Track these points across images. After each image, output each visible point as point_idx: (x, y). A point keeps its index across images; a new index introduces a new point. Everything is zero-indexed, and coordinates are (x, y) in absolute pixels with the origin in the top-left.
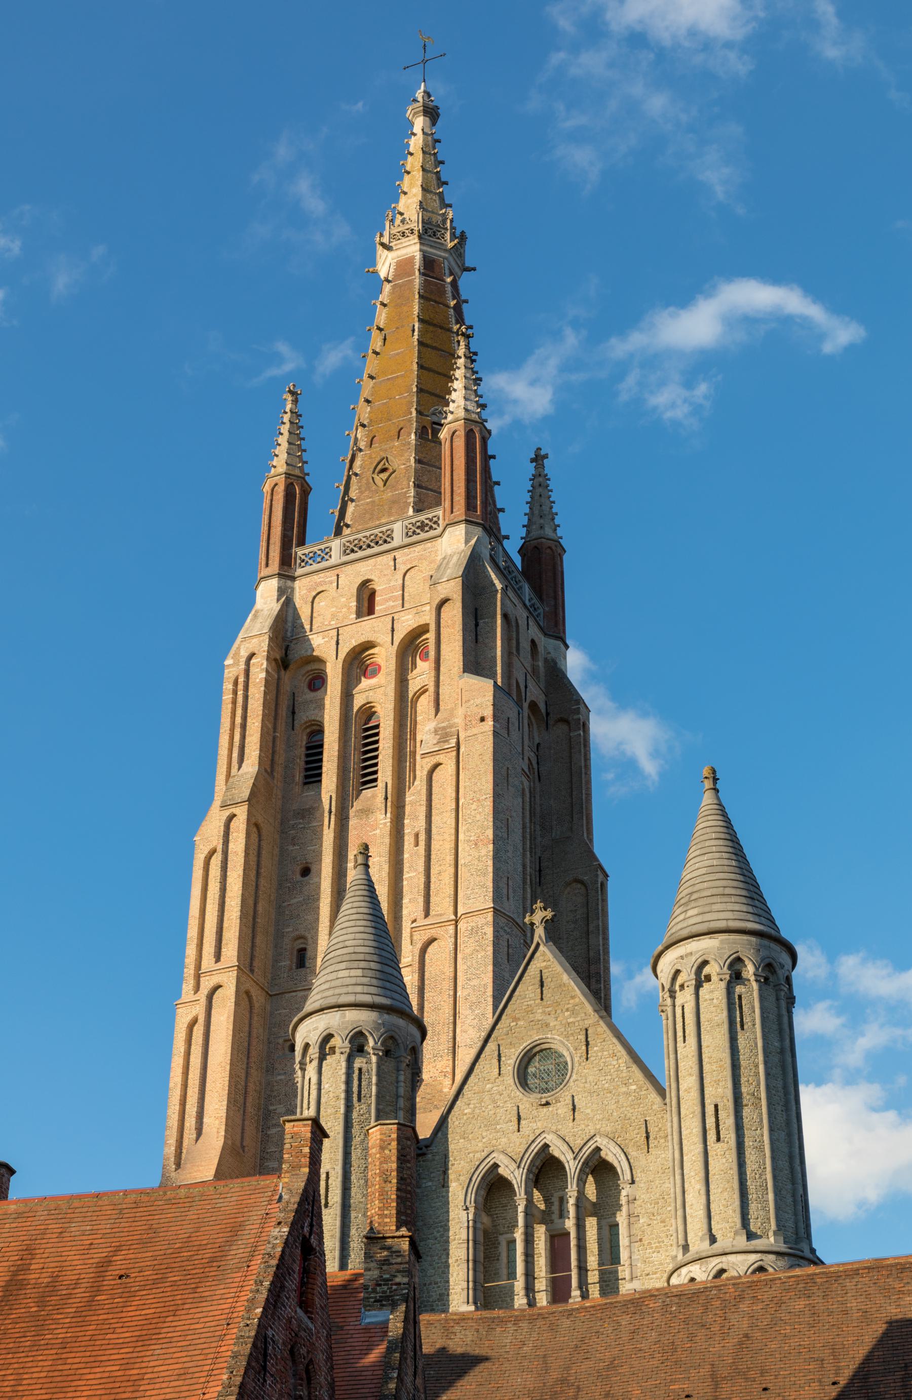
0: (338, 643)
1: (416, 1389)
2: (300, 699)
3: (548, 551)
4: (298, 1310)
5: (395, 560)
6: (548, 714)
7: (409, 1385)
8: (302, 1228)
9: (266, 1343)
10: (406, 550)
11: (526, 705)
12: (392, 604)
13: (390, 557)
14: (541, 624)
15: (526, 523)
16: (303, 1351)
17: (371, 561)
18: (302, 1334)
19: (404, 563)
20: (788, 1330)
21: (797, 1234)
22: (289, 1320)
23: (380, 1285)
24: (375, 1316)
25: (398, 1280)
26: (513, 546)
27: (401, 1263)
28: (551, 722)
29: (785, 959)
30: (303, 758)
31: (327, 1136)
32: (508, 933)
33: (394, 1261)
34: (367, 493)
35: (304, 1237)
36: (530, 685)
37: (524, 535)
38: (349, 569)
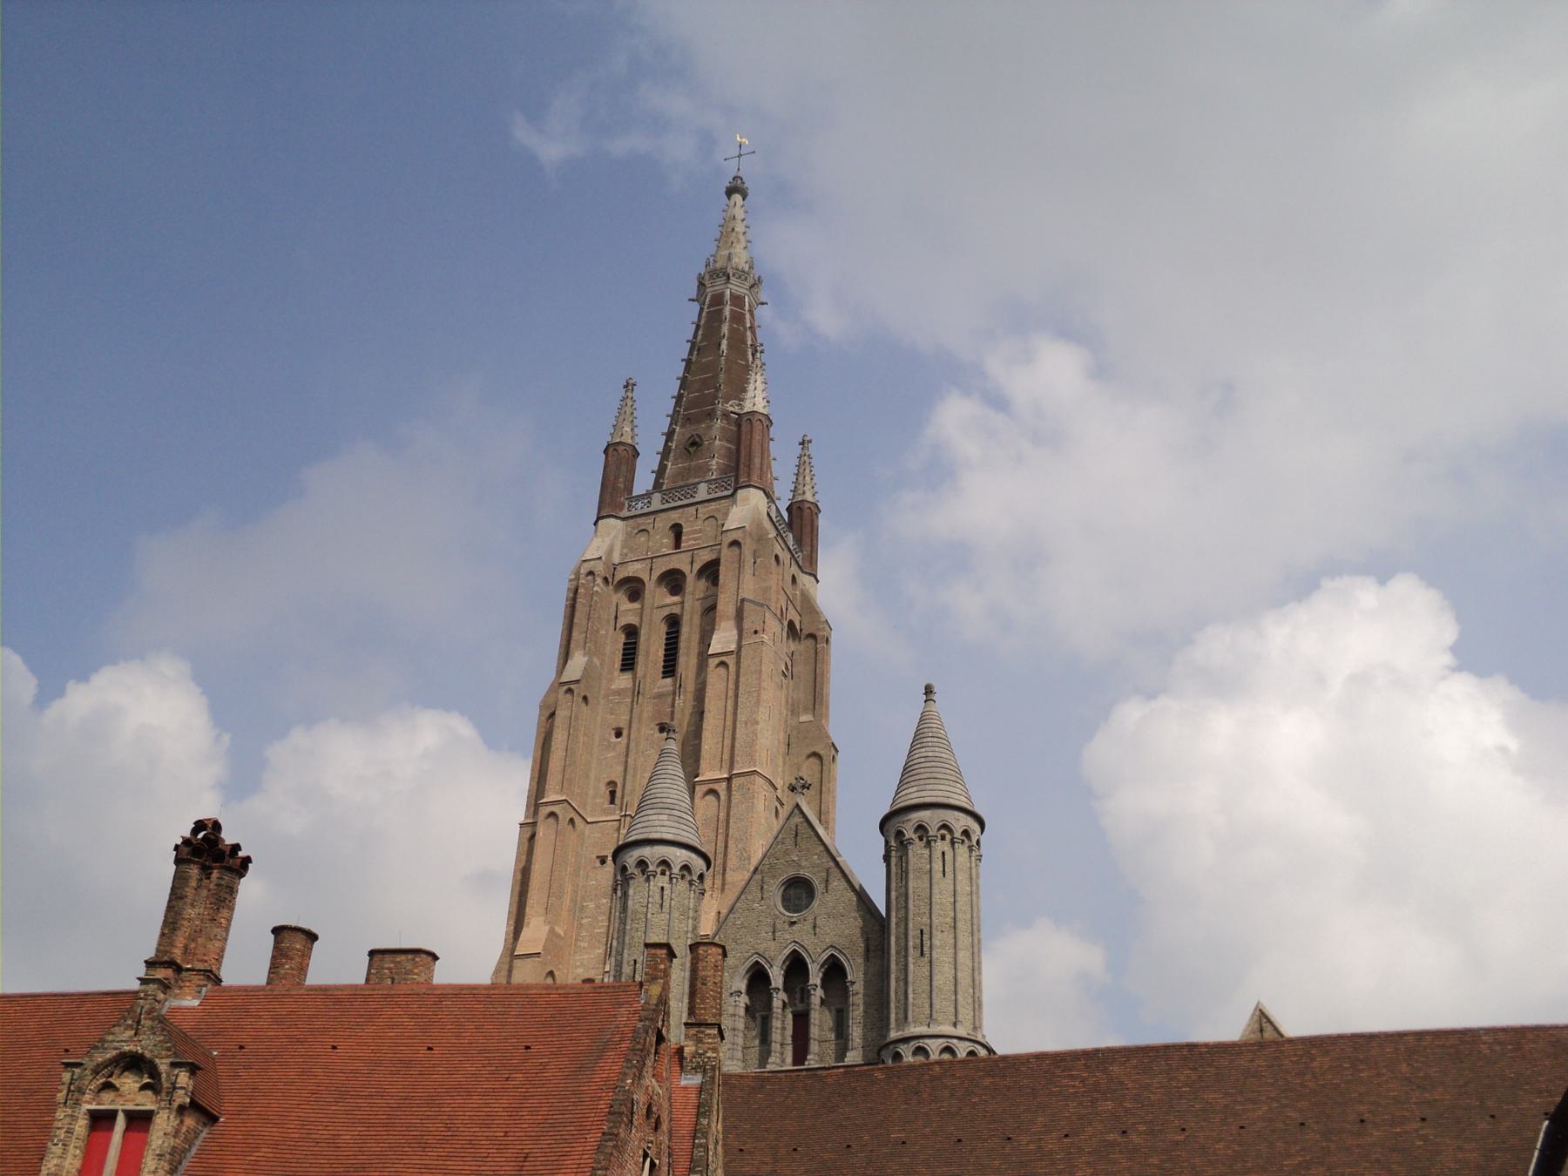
0: (651, 569)
1: (718, 1132)
2: (622, 608)
3: (808, 510)
4: (653, 1080)
5: (697, 510)
6: (801, 630)
7: (714, 1129)
8: (658, 1022)
9: (633, 1104)
10: (706, 504)
11: (786, 623)
12: (694, 542)
13: (694, 508)
14: (800, 563)
15: (793, 489)
16: (654, 1109)
17: (681, 510)
18: (655, 1097)
19: (705, 514)
20: (976, 1100)
21: (974, 1025)
22: (647, 1089)
23: (695, 1058)
24: (693, 1079)
25: (708, 1055)
26: (783, 506)
27: (711, 1043)
28: (803, 636)
29: (975, 826)
30: (621, 652)
31: (676, 957)
32: (765, 790)
33: (706, 1041)
34: (680, 461)
35: (658, 1029)
36: (789, 609)
37: (791, 498)
38: (663, 515)
